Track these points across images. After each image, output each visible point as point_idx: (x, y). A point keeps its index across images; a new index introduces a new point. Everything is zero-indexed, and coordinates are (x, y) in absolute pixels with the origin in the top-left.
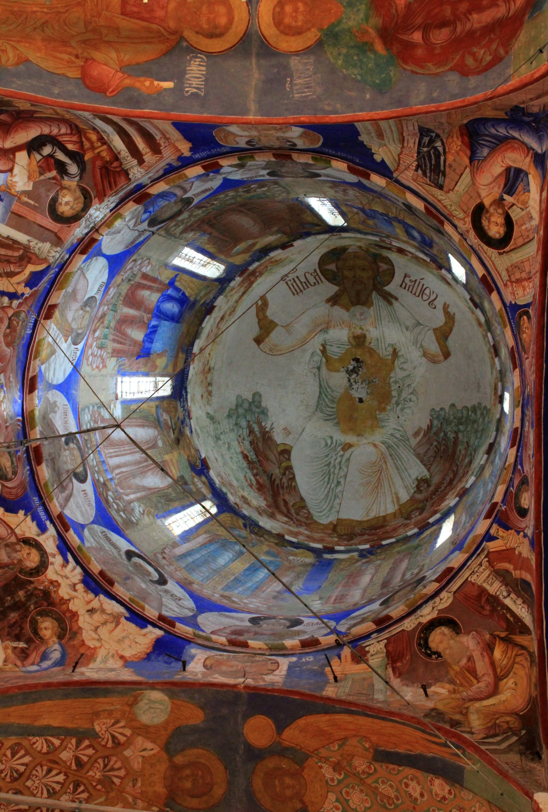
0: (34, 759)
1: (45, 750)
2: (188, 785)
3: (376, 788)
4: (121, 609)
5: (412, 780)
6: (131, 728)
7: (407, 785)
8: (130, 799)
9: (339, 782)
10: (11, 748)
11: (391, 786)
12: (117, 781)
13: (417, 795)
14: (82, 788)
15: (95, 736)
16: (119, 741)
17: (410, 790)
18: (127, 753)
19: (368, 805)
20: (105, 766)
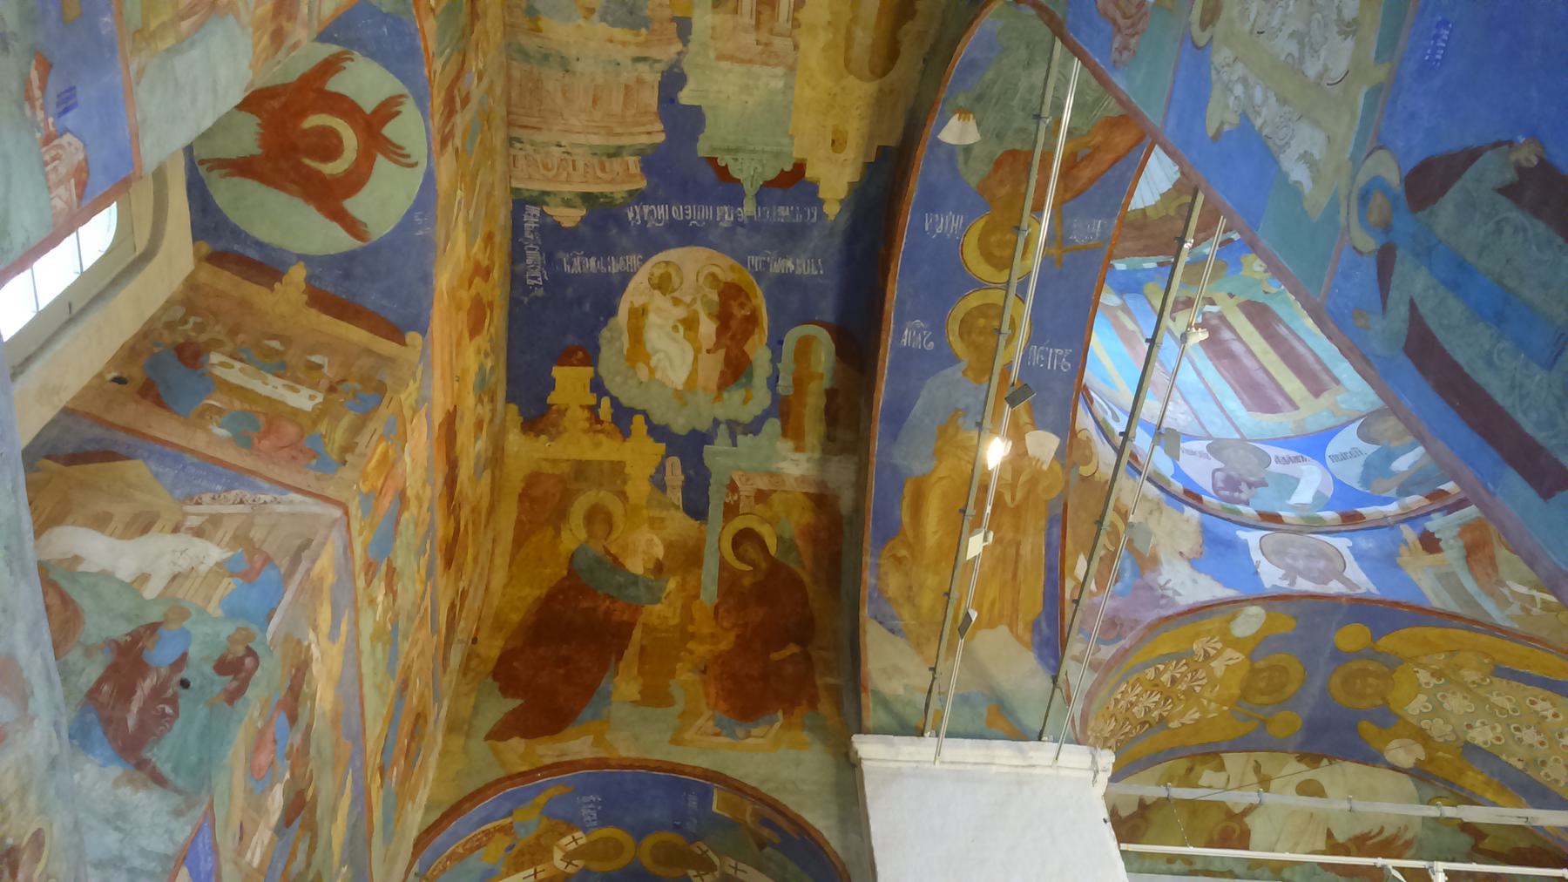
2: (1262, 685)
8: (1205, 702)
11: (1509, 700)
12: (1198, 689)
13: (1549, 714)
14: (1170, 701)
16: (1209, 654)
19: (1469, 710)
20: (1192, 678)
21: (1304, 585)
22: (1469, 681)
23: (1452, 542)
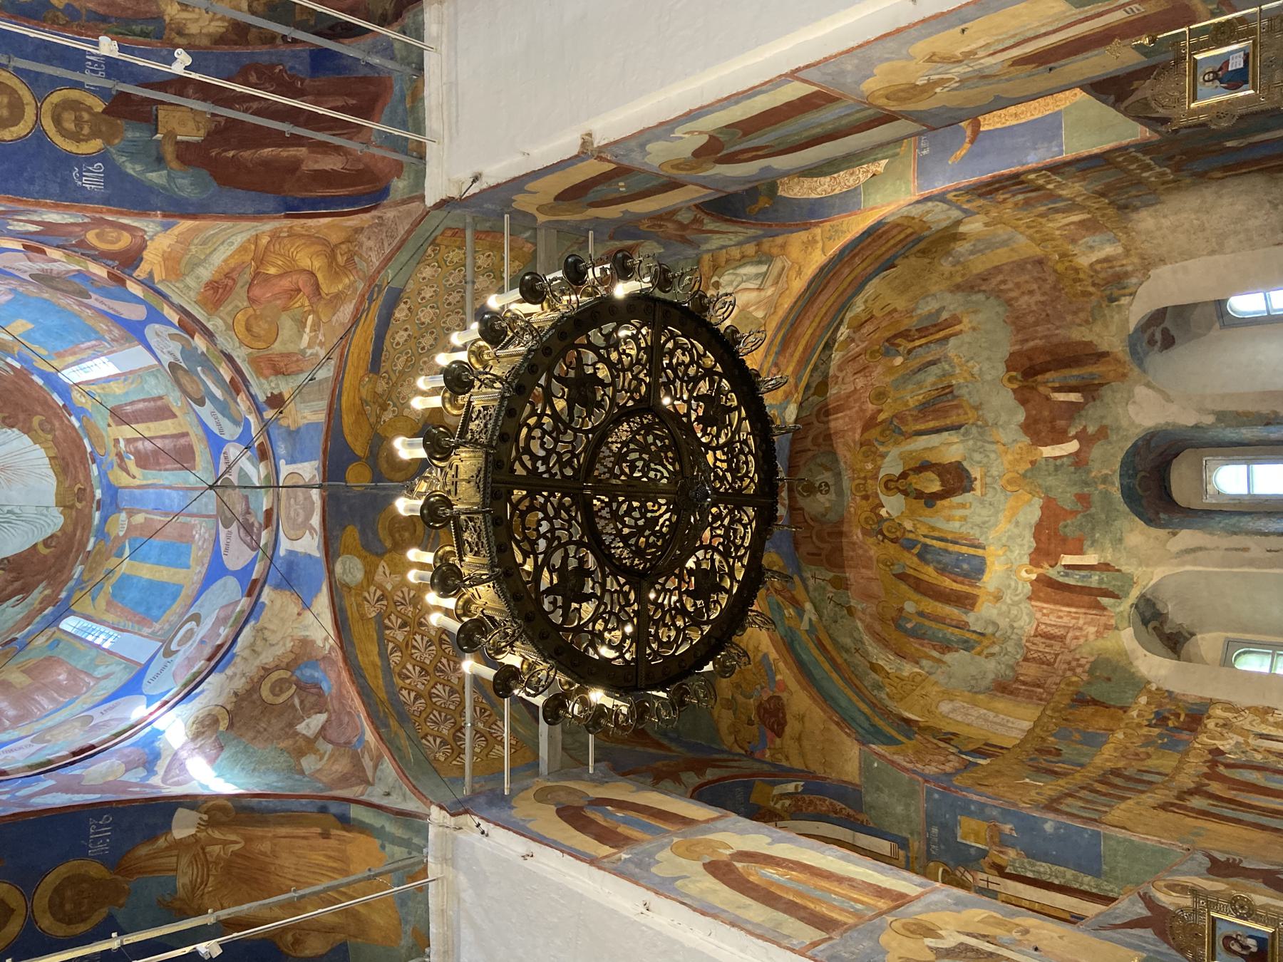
0: (408, 661)
1: (399, 654)
3: (400, 372)
4: (247, 630)
5: (394, 339)
6: (368, 586)
7: (398, 344)
9: (395, 405)
10: (403, 679)
11: (398, 359)
13: (405, 334)
15: (380, 615)
17: (401, 341)
18: (389, 587)
20: (402, 604)
21: (316, 521)
22: (385, 386)
23: (273, 385)
